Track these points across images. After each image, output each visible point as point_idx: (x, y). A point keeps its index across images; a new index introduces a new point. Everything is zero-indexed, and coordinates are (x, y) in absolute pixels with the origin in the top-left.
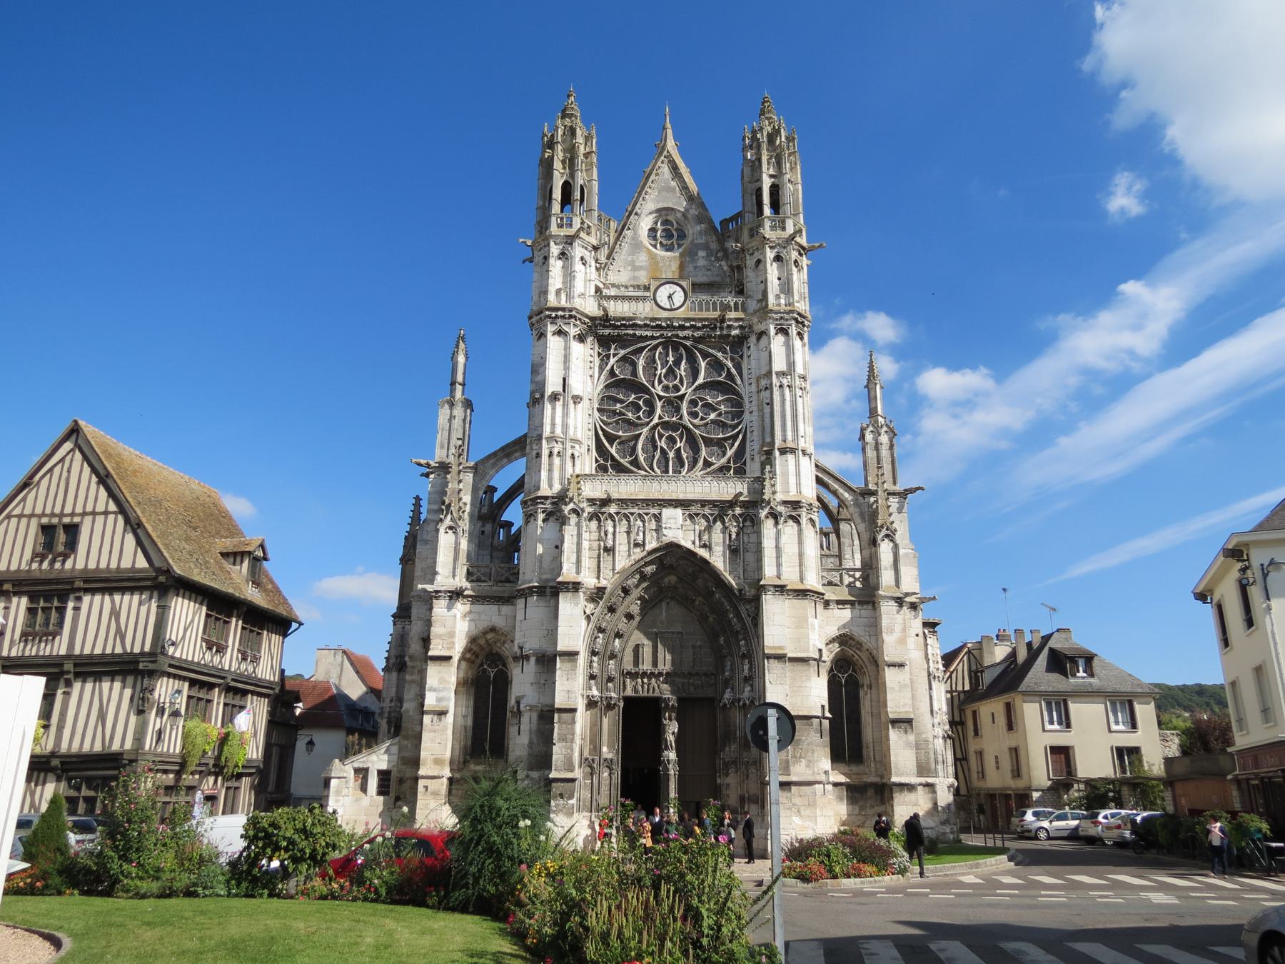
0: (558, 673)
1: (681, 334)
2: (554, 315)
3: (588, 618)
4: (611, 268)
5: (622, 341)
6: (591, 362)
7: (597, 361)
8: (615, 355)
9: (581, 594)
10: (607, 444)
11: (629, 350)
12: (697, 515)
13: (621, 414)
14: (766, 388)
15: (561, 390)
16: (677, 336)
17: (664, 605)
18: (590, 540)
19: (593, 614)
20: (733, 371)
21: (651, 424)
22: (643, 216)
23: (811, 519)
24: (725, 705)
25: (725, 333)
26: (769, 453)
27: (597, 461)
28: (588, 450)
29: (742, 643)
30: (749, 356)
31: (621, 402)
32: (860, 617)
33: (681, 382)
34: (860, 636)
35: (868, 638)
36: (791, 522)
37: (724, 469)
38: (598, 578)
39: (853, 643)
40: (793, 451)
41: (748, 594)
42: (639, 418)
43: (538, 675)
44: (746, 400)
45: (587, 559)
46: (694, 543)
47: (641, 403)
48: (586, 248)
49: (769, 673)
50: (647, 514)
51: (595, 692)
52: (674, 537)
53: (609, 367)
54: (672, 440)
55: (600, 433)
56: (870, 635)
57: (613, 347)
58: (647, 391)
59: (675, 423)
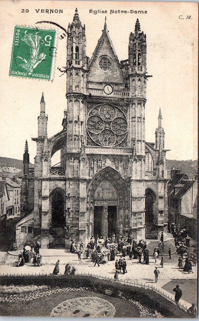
15: (77, 120)
26: (134, 141)
40: (140, 141)
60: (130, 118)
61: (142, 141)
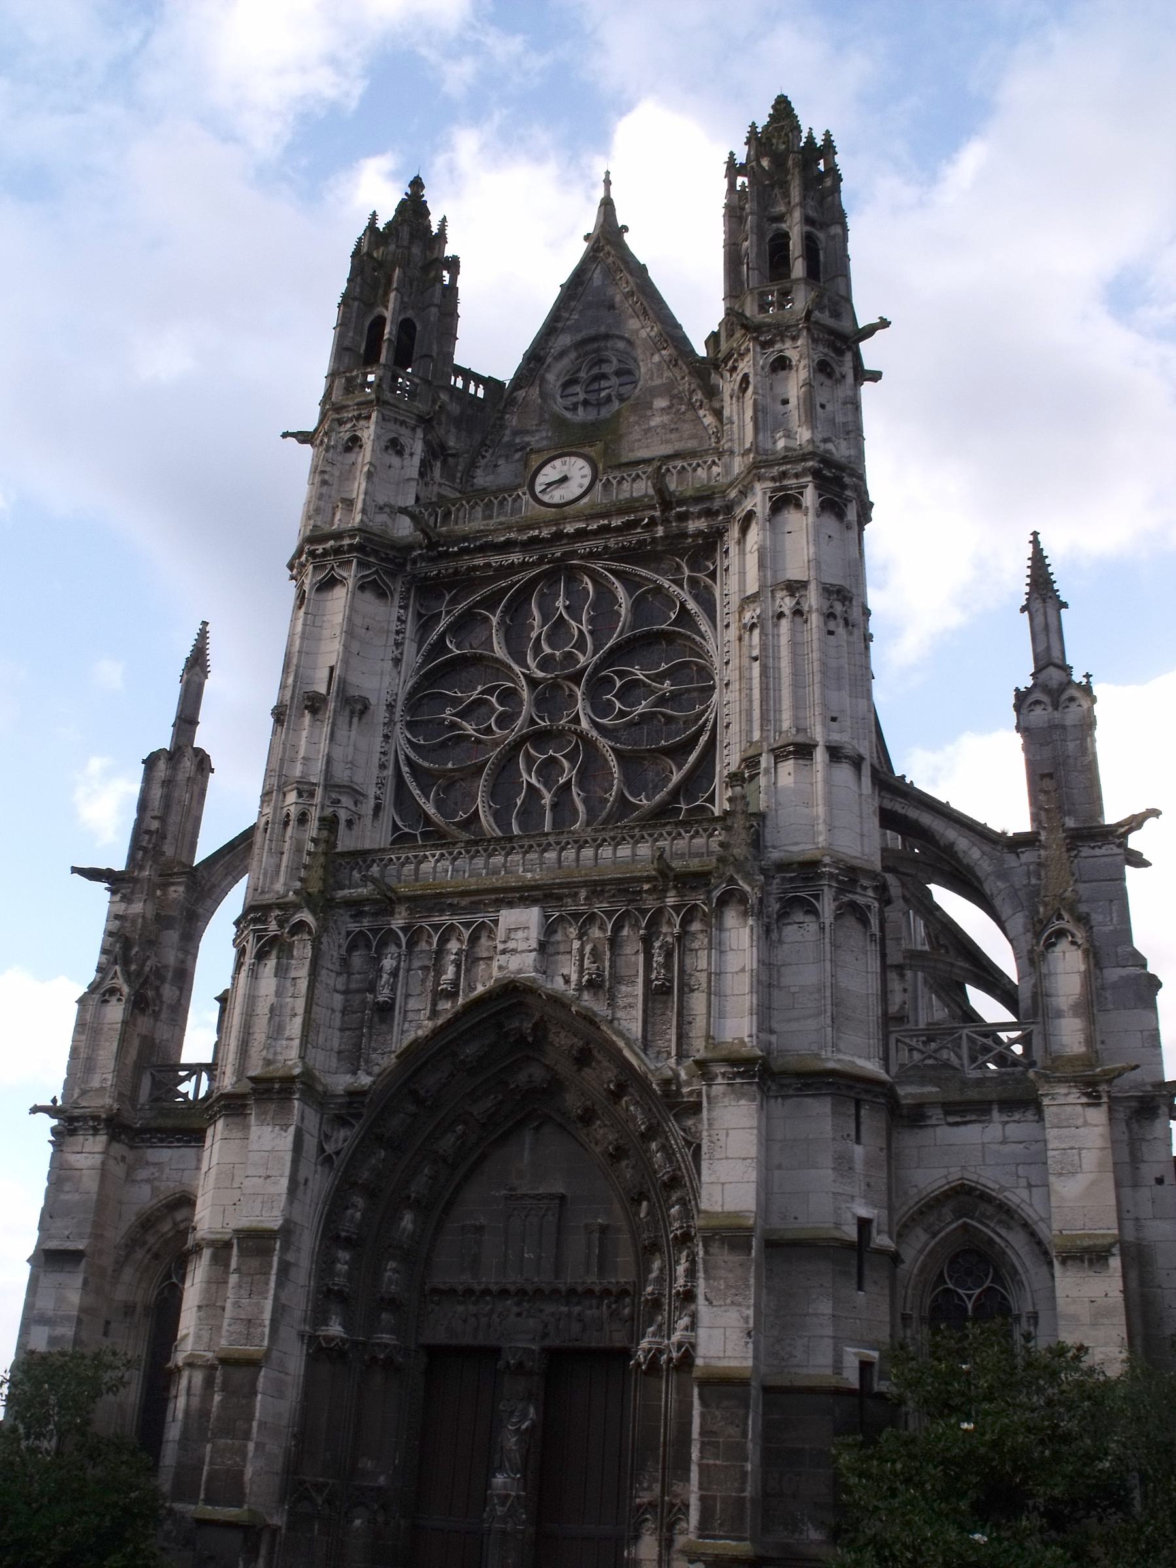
0: (233, 1279)
1: (582, 547)
2: (320, 551)
3: (328, 1160)
4: (483, 462)
5: (464, 582)
6: (398, 632)
7: (410, 628)
8: (448, 613)
9: (296, 1103)
10: (416, 792)
11: (477, 597)
12: (576, 916)
13: (454, 726)
14: (753, 626)
16: (573, 554)
17: (528, 1137)
18: (346, 992)
19: (338, 1153)
20: (692, 605)
21: (511, 738)
22: (549, 360)
23: (853, 905)
24: (639, 1365)
25: (675, 531)
27: (395, 827)
28: (378, 808)
29: (674, 1210)
30: (727, 570)
31: (455, 701)
32: (1004, 1142)
33: (581, 645)
34: (1003, 1189)
35: (1024, 1194)
36: (799, 916)
37: (663, 814)
38: (354, 1073)
39: (990, 1210)
41: (685, 1090)
42: (488, 730)
43: (214, 1287)
44: (717, 662)
45: (337, 1033)
46: (567, 981)
47: (494, 700)
48: (403, 423)
49: (707, 1279)
50: (467, 925)
51: (335, 1329)
52: (520, 971)
53: (434, 636)
54: (548, 769)
55: (405, 769)
56: (1030, 1186)
57: (447, 598)
58: (509, 675)
59: (561, 733)
60: (733, 619)
61: (820, 755)
